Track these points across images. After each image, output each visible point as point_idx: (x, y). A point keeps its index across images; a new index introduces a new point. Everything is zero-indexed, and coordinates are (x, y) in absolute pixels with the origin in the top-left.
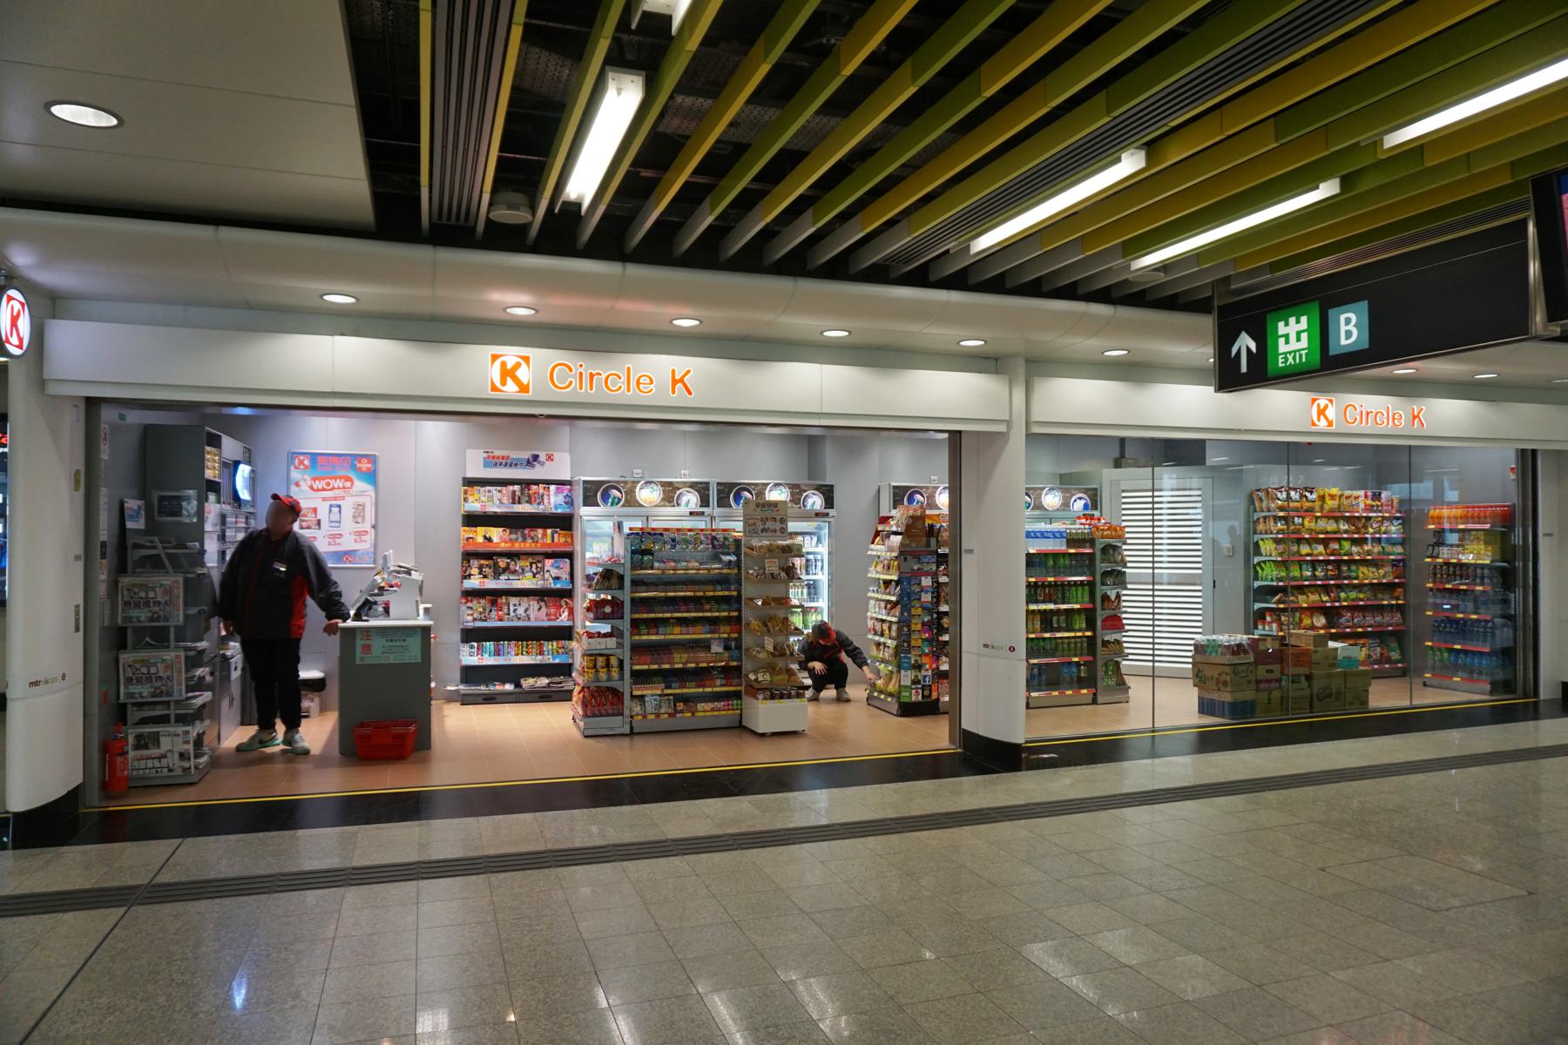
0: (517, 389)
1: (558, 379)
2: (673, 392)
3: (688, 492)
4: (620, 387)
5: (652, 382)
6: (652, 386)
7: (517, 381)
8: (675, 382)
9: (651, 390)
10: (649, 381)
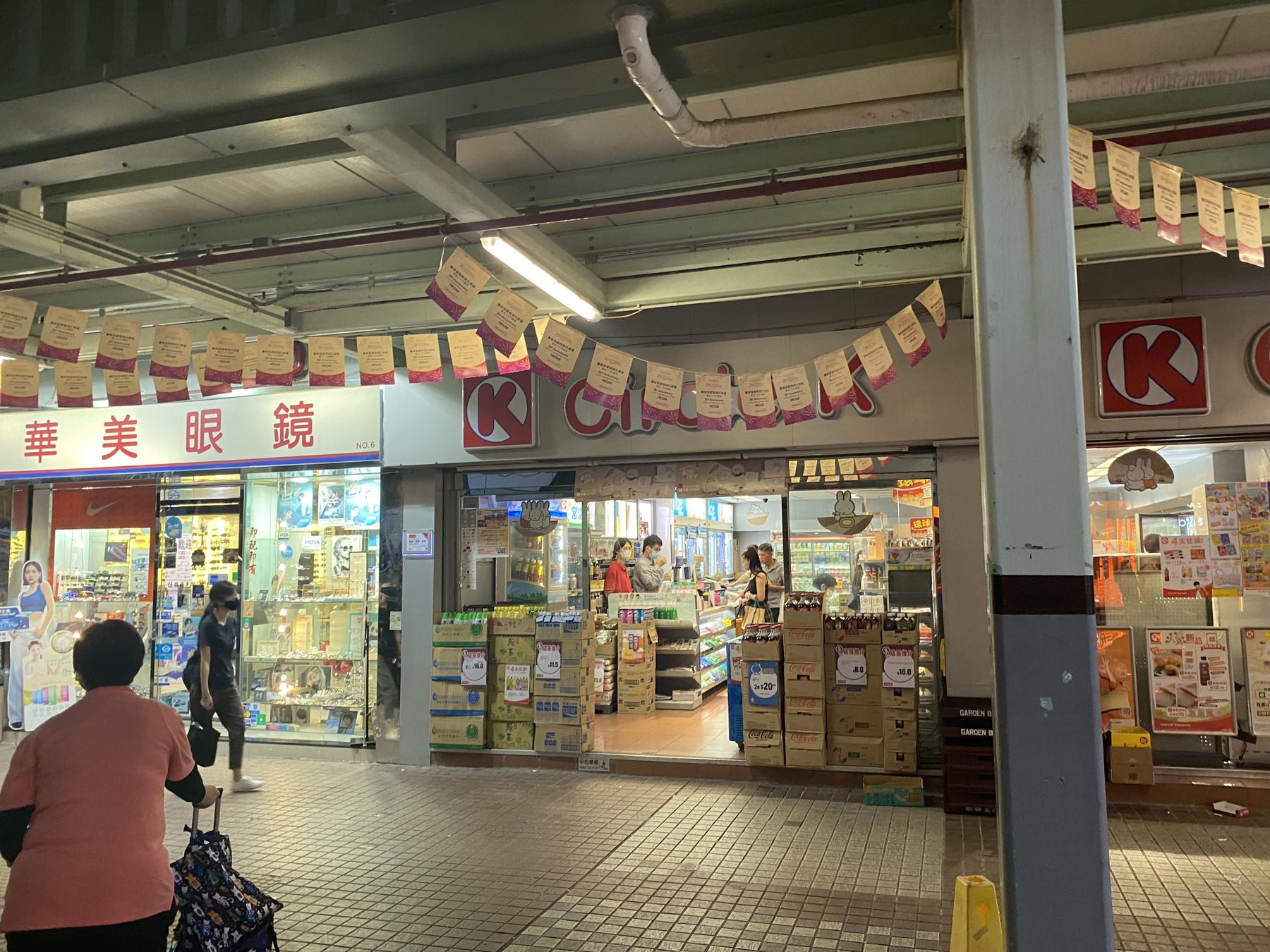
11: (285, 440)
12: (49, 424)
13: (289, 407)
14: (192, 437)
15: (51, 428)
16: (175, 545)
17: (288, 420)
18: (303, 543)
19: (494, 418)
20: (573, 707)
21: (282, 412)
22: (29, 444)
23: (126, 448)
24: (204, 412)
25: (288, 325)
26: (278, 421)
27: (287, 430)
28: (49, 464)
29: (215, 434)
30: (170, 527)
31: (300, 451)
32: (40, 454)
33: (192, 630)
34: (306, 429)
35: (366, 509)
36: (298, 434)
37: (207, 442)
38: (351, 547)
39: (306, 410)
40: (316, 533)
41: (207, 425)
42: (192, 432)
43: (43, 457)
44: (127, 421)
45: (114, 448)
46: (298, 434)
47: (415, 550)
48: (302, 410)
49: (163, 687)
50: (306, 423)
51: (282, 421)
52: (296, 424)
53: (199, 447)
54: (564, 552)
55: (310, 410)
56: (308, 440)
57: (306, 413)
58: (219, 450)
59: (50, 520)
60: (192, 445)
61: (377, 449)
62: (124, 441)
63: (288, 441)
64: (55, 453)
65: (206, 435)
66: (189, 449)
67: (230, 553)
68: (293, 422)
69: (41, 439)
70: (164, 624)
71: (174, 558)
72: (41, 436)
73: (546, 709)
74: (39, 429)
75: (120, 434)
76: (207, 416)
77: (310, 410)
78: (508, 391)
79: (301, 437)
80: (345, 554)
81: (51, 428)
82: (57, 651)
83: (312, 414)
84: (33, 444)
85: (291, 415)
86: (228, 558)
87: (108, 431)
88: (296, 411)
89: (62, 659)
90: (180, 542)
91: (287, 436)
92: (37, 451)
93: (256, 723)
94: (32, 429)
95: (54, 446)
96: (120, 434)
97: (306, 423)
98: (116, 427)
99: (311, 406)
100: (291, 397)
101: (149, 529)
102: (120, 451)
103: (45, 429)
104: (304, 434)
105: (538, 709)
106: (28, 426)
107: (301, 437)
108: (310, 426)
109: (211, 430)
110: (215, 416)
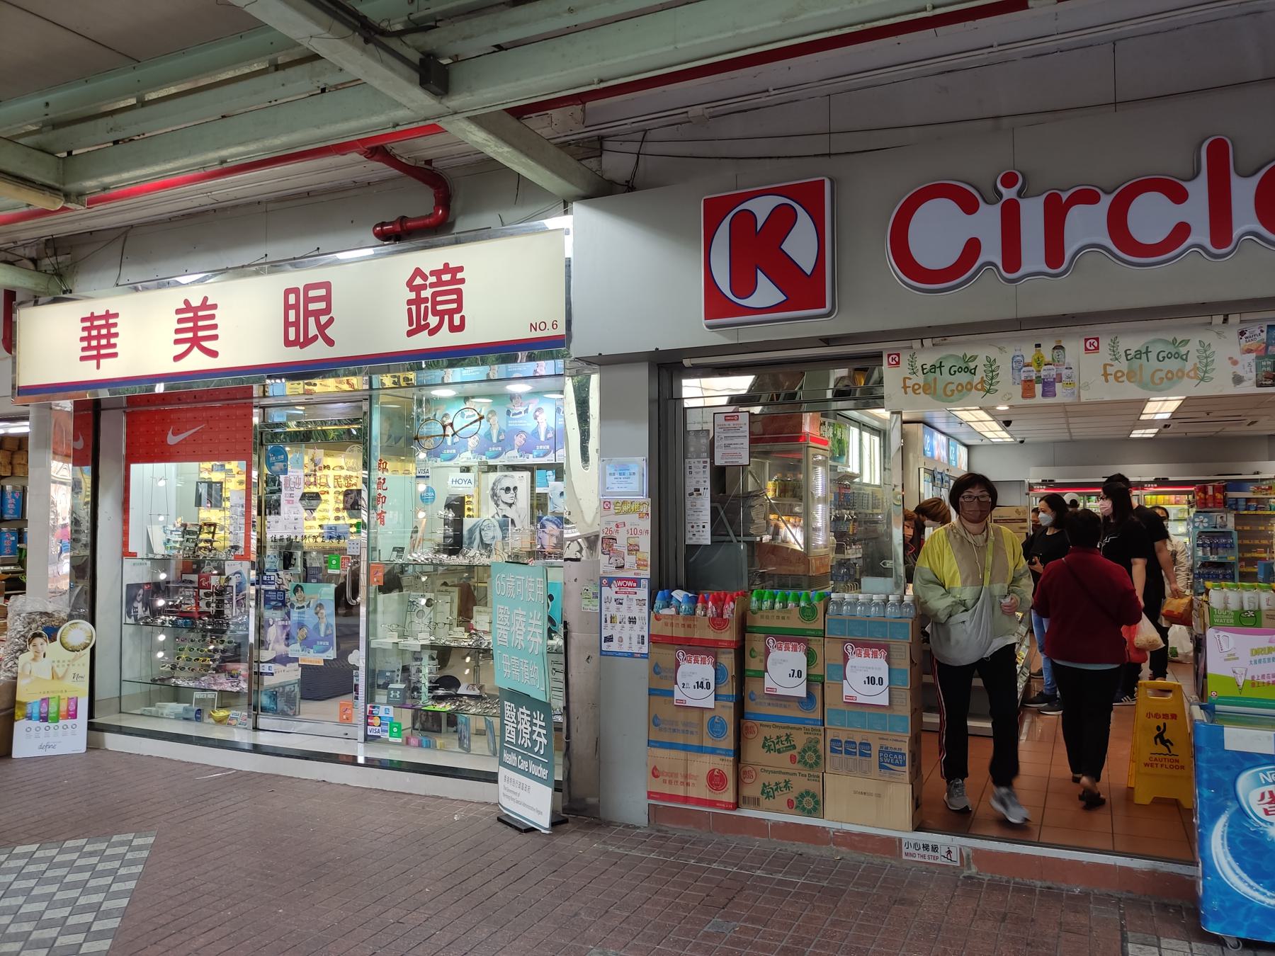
0: (781, 298)
7: (784, 272)
11: (423, 323)
12: (108, 316)
13: (428, 275)
14: (292, 324)
15: (111, 321)
16: (279, 484)
17: (426, 293)
18: (450, 480)
19: (757, 267)
20: (898, 754)
21: (418, 281)
22: (85, 344)
23: (205, 344)
24: (308, 287)
25: (424, 83)
26: (413, 296)
27: (426, 308)
28: (110, 369)
29: (324, 319)
30: (272, 459)
31: (445, 339)
32: (98, 357)
33: (304, 600)
34: (454, 306)
35: (536, 433)
36: (441, 314)
37: (313, 330)
38: (515, 488)
39: (454, 276)
40: (466, 469)
41: (312, 307)
42: (292, 318)
43: (102, 361)
44: (204, 306)
45: (188, 345)
46: (441, 314)
47: (616, 490)
48: (446, 277)
49: (266, 677)
50: (454, 297)
51: (418, 295)
52: (439, 299)
53: (302, 340)
54: (825, 500)
55: (459, 276)
56: (457, 322)
57: (454, 281)
58: (330, 342)
59: (124, 452)
60: (292, 337)
61: (561, 330)
62: (201, 334)
63: (428, 325)
64: (115, 355)
65: (312, 320)
66: (288, 343)
67: (353, 495)
68: (435, 295)
69: (99, 337)
70: (266, 591)
71: (278, 503)
72: (99, 332)
73: (848, 752)
74: (96, 323)
75: (196, 324)
76: (312, 293)
77: (459, 276)
78: (782, 221)
79: (446, 317)
80: (507, 497)
81: (111, 321)
82: (68, 649)
83: (462, 281)
84: (89, 344)
85: (432, 285)
86: (351, 501)
87: (180, 321)
88: (439, 278)
89: (74, 660)
90: (286, 480)
91: (426, 318)
92: (95, 353)
93: (388, 734)
94: (88, 324)
95: (114, 346)
96: (196, 324)
97: (454, 297)
98: (191, 315)
99: (461, 269)
100: (431, 259)
101: (245, 462)
102: (195, 349)
103: (103, 322)
104: (451, 313)
105: (833, 750)
106: (83, 320)
107: (446, 317)
108: (459, 301)
109: (316, 314)
110: (322, 292)
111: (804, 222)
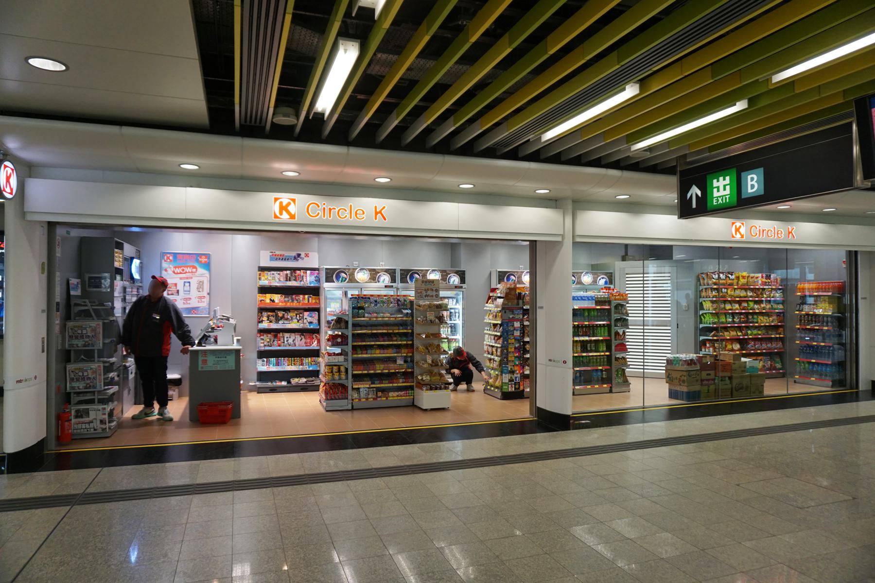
1: (311, 211)
2: (376, 219)
3: (384, 274)
4: (346, 216)
5: (364, 213)
6: (364, 216)
8: (376, 213)
9: (364, 218)
10: (362, 213)
78: (289, 204)
111: (292, 202)
